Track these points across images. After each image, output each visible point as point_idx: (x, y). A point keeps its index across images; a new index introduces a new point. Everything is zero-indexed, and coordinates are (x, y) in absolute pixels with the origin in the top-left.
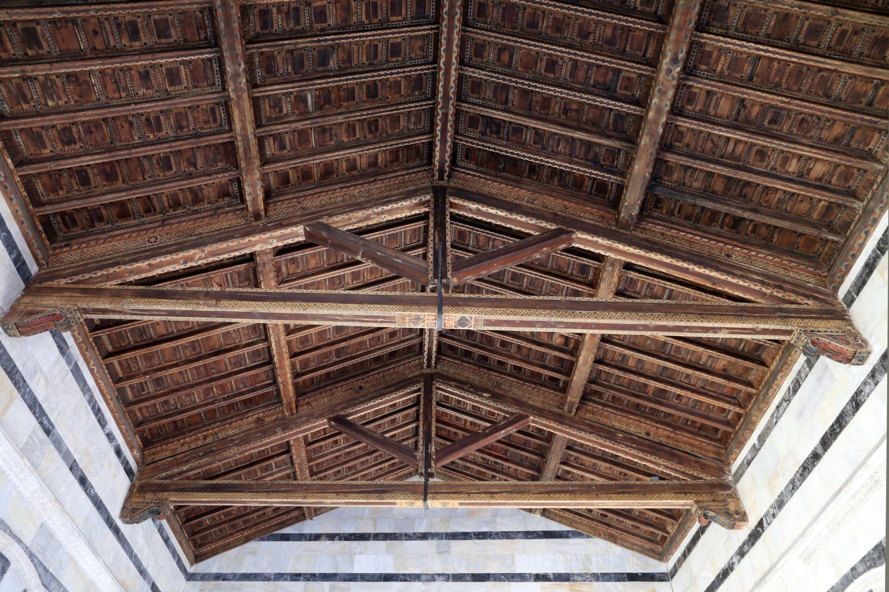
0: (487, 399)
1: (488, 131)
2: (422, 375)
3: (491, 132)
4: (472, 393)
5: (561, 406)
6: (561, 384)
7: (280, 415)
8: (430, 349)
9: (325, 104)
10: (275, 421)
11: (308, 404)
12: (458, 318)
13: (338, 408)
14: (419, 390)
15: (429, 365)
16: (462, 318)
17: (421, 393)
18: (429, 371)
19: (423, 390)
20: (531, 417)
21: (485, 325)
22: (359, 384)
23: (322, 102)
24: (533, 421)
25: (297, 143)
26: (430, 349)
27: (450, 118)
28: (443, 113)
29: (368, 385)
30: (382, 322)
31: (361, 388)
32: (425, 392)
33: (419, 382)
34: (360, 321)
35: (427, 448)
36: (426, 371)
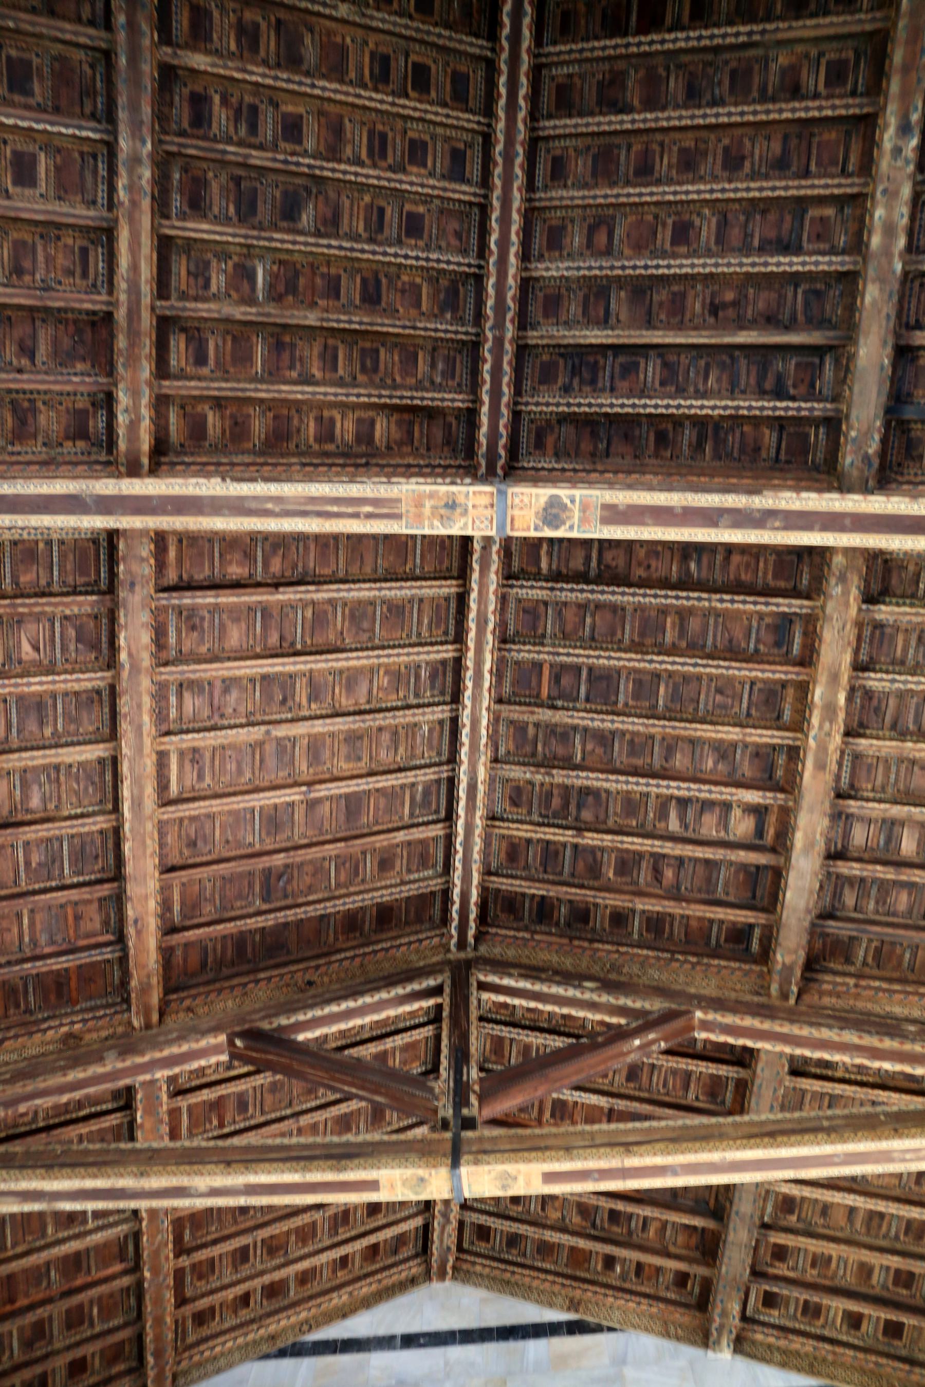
0: (592, 990)
1: (576, 382)
2: (449, 962)
3: (581, 382)
4: (559, 983)
5: (763, 990)
6: (755, 946)
7: (120, 1030)
8: (465, 896)
9: (287, 292)
10: (106, 1039)
11: (189, 1009)
12: (543, 501)
13: (257, 1016)
14: (437, 991)
15: (462, 944)
16: (554, 503)
17: (445, 1000)
18: (462, 955)
19: (447, 990)
20: (699, 1014)
21: (605, 521)
22: (307, 977)
23: (281, 288)
24: (706, 1026)
25: (228, 358)
26: (465, 896)
27: (507, 346)
28: (495, 337)
29: (326, 979)
30: (369, 516)
31: (310, 983)
32: (453, 996)
33: (441, 972)
34: (319, 514)
35: (458, 1073)
36: (455, 954)
